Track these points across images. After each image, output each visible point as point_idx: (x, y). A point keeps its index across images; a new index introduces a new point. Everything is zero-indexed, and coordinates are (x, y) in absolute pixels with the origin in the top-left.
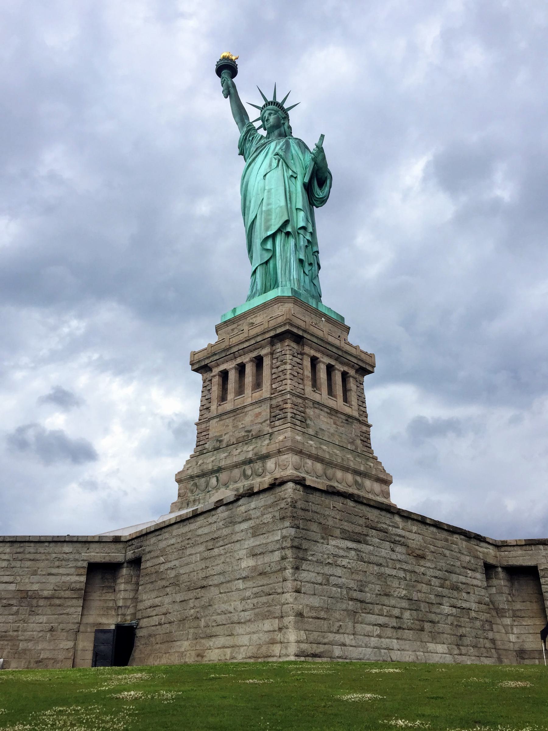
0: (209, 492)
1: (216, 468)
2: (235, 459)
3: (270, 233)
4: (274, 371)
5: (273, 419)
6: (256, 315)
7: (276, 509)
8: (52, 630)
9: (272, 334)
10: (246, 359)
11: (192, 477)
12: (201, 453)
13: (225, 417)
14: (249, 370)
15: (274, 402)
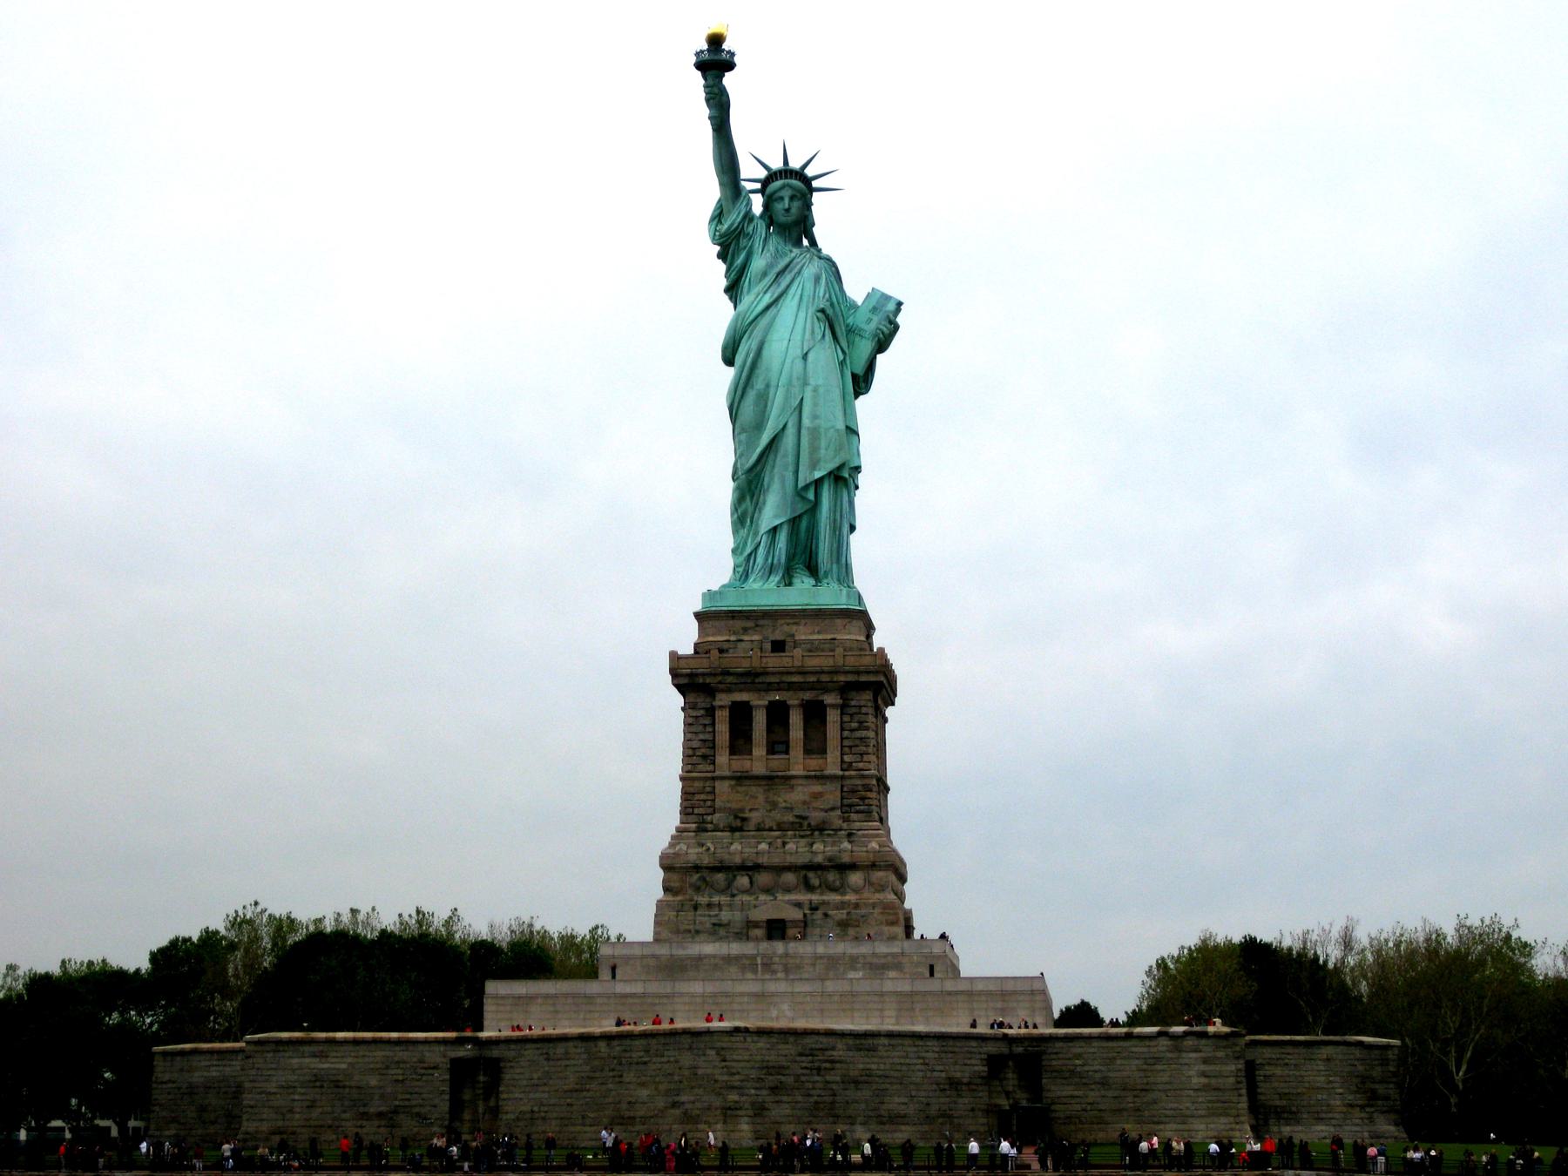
0: (733, 896)
1: (750, 864)
2: (790, 859)
3: (818, 475)
4: (846, 733)
5: (847, 808)
6: (795, 621)
7: (1229, 1050)
8: (973, 1110)
9: (850, 678)
10: (793, 699)
11: (697, 868)
12: (701, 829)
13: (748, 782)
14: (796, 720)
15: (845, 783)
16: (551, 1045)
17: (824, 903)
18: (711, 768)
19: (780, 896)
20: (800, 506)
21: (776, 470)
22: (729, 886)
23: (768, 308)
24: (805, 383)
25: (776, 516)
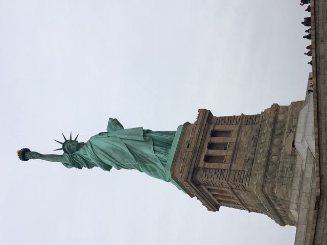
1: (267, 154)
2: (268, 140)
3: (142, 134)
9: (206, 120)
10: (208, 139)
11: (265, 176)
14: (215, 140)
15: (243, 124)
16: (323, 112)
17: (289, 127)
18: (226, 171)
19: (284, 144)
20: (150, 142)
21: (136, 147)
22: (275, 164)
23: (92, 147)
24: (116, 137)
25: (150, 149)
